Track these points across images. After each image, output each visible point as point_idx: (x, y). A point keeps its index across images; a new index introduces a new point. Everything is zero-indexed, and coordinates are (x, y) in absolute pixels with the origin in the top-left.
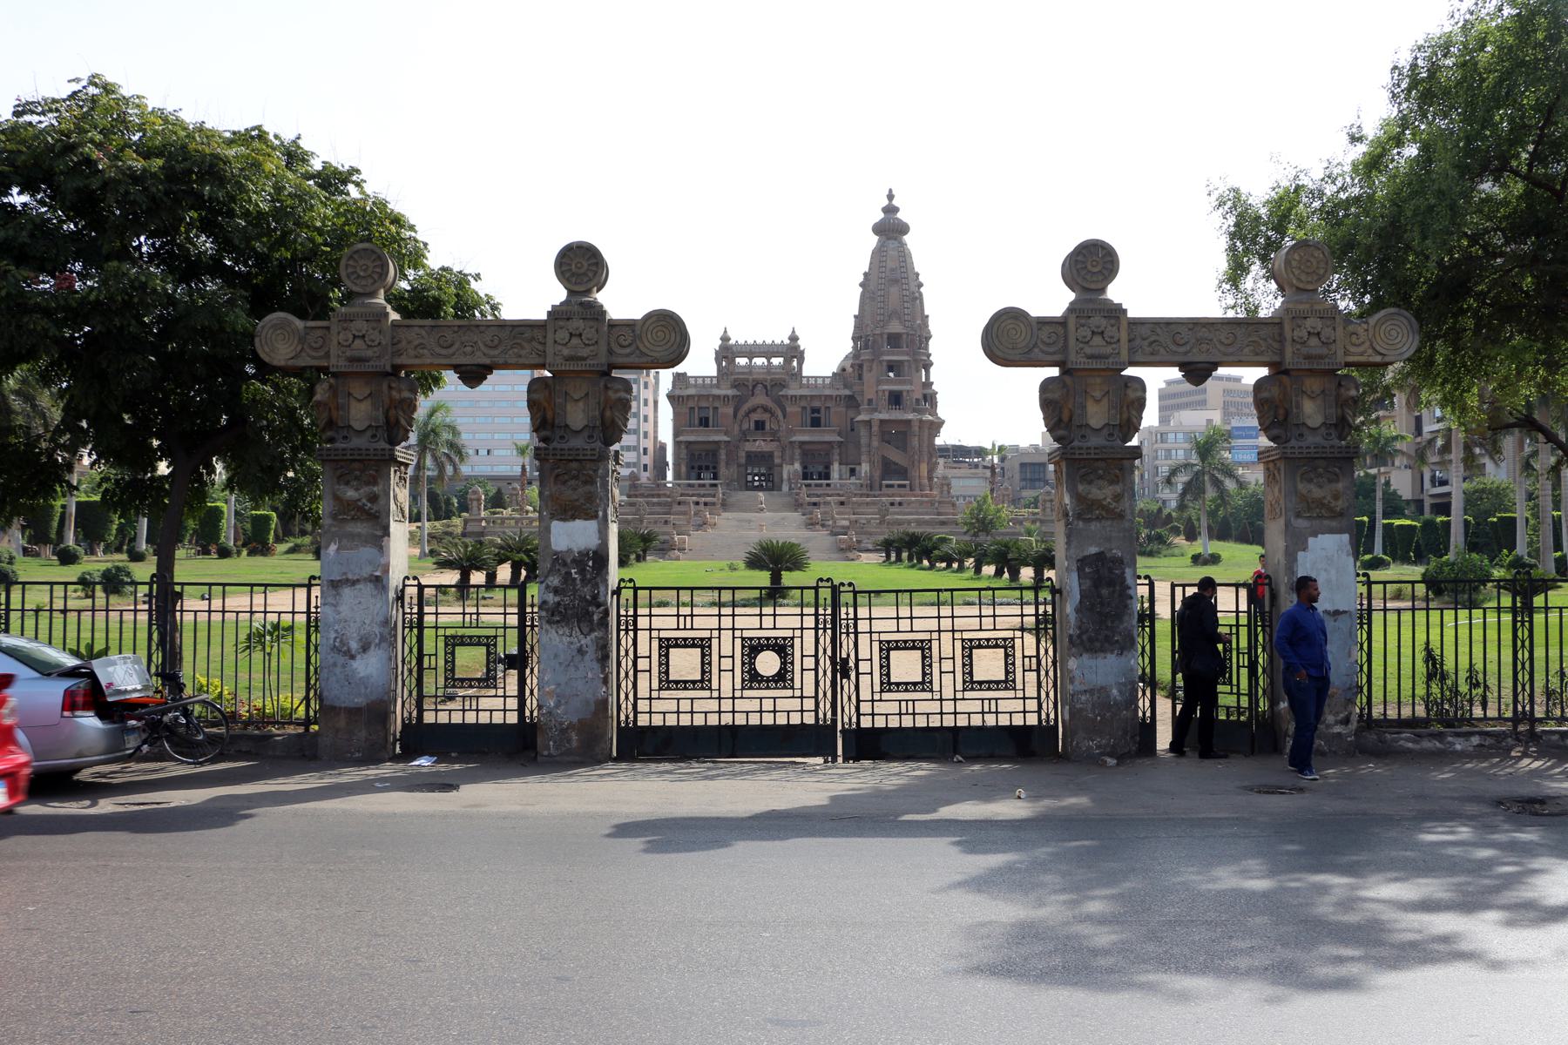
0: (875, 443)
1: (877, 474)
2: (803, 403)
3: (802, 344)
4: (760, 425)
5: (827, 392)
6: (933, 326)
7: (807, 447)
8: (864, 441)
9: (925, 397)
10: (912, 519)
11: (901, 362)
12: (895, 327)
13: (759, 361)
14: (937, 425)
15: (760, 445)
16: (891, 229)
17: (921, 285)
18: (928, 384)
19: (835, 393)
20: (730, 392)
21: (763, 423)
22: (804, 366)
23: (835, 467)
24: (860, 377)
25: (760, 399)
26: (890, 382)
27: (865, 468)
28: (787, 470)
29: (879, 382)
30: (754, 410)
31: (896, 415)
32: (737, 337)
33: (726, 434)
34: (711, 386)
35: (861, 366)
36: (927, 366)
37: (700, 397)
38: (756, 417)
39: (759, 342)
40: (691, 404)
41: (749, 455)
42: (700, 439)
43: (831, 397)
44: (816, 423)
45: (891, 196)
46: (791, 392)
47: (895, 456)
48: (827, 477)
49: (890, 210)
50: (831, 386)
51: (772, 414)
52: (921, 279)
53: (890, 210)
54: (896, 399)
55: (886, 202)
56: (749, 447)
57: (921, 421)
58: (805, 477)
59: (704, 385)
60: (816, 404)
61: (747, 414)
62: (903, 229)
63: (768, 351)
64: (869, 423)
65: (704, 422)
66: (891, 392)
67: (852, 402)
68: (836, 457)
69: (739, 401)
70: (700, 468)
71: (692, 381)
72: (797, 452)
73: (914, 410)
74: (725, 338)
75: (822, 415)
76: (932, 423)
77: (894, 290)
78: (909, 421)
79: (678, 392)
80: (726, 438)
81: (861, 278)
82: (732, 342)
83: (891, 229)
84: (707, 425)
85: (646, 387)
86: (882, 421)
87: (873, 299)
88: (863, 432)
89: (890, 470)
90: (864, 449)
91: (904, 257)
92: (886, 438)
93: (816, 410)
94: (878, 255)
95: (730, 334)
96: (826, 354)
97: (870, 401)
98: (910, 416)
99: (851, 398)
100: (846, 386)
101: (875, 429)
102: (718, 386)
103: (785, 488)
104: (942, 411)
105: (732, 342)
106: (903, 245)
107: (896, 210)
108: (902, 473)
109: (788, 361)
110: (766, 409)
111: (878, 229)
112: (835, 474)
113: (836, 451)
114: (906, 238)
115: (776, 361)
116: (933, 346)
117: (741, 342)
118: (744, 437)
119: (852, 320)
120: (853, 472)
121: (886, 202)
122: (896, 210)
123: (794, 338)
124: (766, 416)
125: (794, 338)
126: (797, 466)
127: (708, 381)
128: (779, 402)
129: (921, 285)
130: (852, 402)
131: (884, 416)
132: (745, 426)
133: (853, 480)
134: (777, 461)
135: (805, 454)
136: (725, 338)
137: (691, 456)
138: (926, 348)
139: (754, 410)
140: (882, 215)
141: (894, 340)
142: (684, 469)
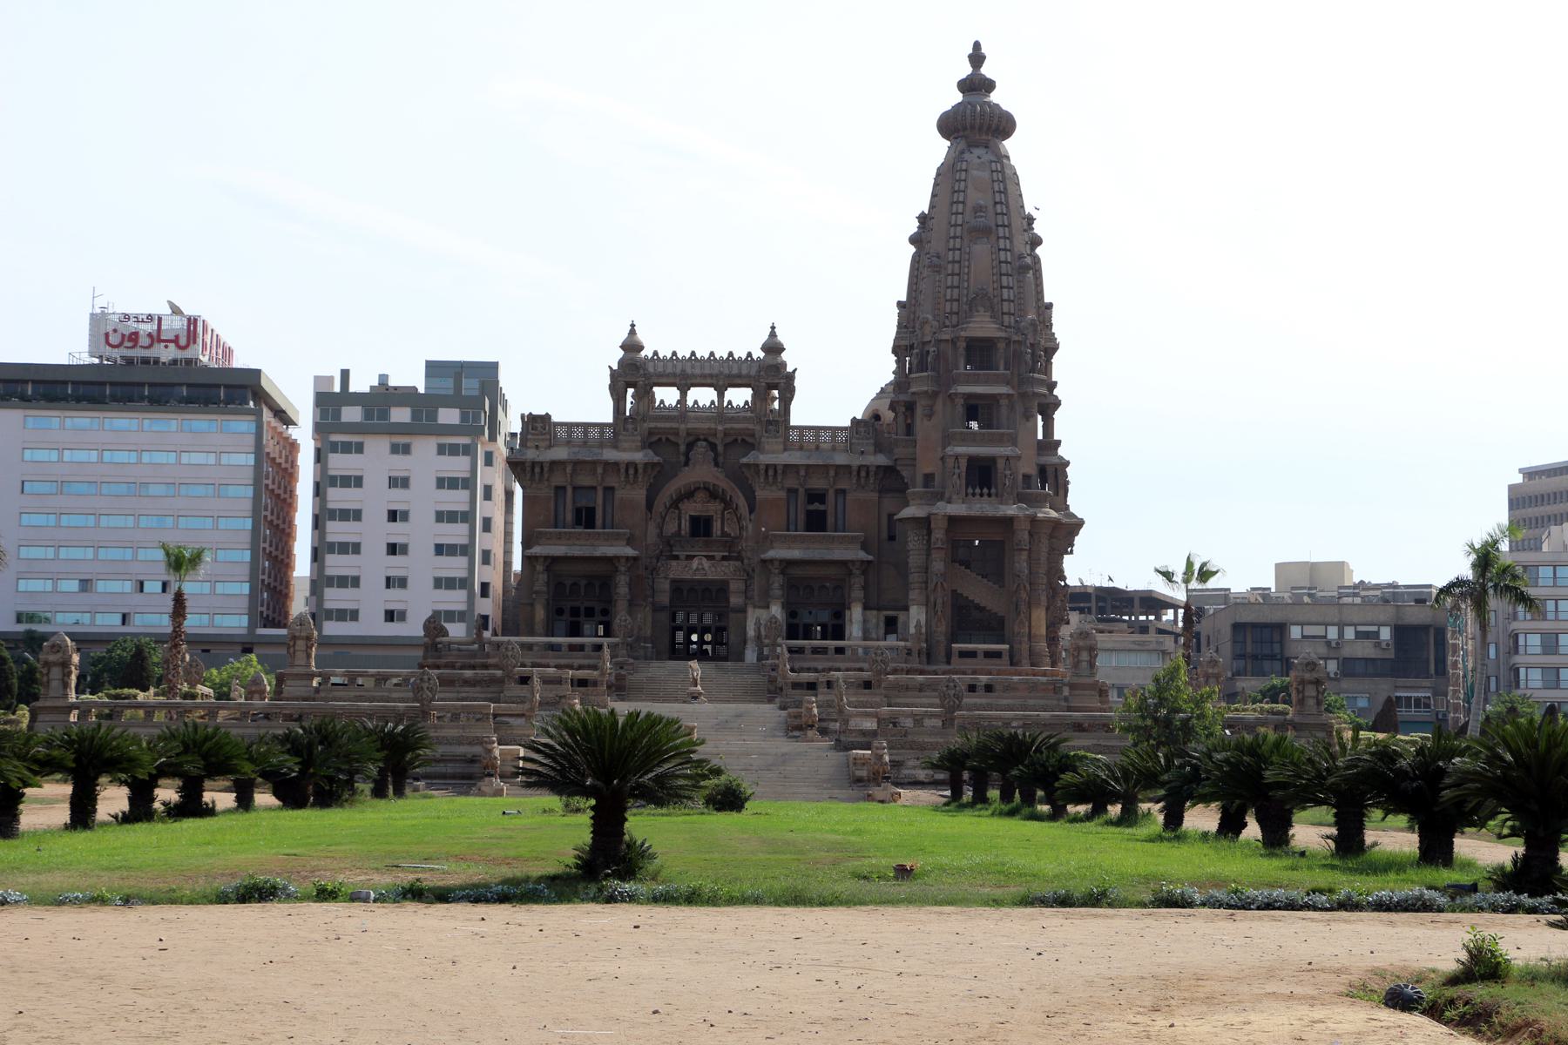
0: (938, 566)
1: (942, 629)
2: (791, 482)
3: (790, 359)
4: (701, 527)
5: (841, 459)
6: (1060, 326)
7: (797, 572)
8: (915, 560)
9: (1042, 470)
10: (1010, 713)
11: (994, 398)
12: (982, 326)
13: (702, 396)
14: (1067, 531)
15: (701, 567)
16: (976, 125)
17: (1037, 241)
18: (1051, 445)
19: (856, 461)
20: (639, 457)
21: (708, 522)
22: (795, 407)
23: (856, 614)
24: (909, 430)
25: (702, 471)
26: (973, 438)
27: (916, 616)
28: (754, 619)
29: (947, 439)
30: (689, 494)
31: (983, 507)
32: (658, 343)
33: (630, 541)
34: (601, 444)
35: (910, 407)
36: (1049, 407)
37: (577, 464)
38: (692, 508)
39: (702, 353)
40: (558, 479)
41: (677, 586)
42: (576, 551)
44: (816, 522)
45: (977, 58)
46: (764, 459)
47: (979, 592)
48: (838, 632)
49: (976, 85)
50: (850, 447)
51: (728, 504)
52: (1038, 228)
53: (976, 85)
54: (982, 475)
55: (967, 70)
56: (677, 570)
57: (1033, 520)
58: (792, 633)
60: (817, 483)
61: (675, 504)
62: (1003, 125)
63: (721, 373)
64: (925, 523)
65: (585, 518)
66: (973, 461)
67: (891, 480)
68: (857, 593)
69: (657, 475)
70: (575, 612)
71: (562, 433)
72: (777, 582)
73: (1020, 498)
74: (631, 346)
75: (829, 506)
76: (1056, 524)
77: (981, 249)
78: (1008, 522)
79: (531, 455)
80: (629, 552)
81: (913, 226)
82: (647, 352)
83: (976, 125)
84: (590, 524)
85: (489, 461)
86: (953, 520)
87: (937, 269)
88: (914, 542)
89: (968, 620)
90: (915, 578)
91: (1004, 183)
92: (960, 555)
93: (816, 497)
94: (948, 179)
95: (641, 336)
96: (842, 382)
97: (928, 478)
98: (1011, 510)
99: (889, 471)
100: (879, 448)
101: (938, 534)
102: (615, 444)
103: (751, 655)
104: (1077, 502)
105: (647, 352)
106: (1003, 158)
107: (989, 85)
108: (994, 627)
109: (761, 396)
110: (713, 494)
111: (949, 125)
112: (854, 629)
113: (858, 581)
114: (1009, 145)
115: (739, 396)
116: (1060, 367)
117: (665, 353)
118: (668, 548)
119: (894, 313)
120: (891, 625)
121: (967, 70)
122: (989, 85)
123: (773, 347)
124: (714, 508)
125: (773, 347)
126: (776, 610)
127: (594, 434)
128: (743, 478)
129: (1037, 241)
130: (891, 480)
131: (957, 509)
132: (671, 528)
133: (892, 641)
134: (735, 600)
135: (792, 586)
136: (631, 346)
137: (558, 589)
138: (1047, 369)
139: (689, 494)
140: (958, 97)
141: (980, 352)
142: (540, 613)
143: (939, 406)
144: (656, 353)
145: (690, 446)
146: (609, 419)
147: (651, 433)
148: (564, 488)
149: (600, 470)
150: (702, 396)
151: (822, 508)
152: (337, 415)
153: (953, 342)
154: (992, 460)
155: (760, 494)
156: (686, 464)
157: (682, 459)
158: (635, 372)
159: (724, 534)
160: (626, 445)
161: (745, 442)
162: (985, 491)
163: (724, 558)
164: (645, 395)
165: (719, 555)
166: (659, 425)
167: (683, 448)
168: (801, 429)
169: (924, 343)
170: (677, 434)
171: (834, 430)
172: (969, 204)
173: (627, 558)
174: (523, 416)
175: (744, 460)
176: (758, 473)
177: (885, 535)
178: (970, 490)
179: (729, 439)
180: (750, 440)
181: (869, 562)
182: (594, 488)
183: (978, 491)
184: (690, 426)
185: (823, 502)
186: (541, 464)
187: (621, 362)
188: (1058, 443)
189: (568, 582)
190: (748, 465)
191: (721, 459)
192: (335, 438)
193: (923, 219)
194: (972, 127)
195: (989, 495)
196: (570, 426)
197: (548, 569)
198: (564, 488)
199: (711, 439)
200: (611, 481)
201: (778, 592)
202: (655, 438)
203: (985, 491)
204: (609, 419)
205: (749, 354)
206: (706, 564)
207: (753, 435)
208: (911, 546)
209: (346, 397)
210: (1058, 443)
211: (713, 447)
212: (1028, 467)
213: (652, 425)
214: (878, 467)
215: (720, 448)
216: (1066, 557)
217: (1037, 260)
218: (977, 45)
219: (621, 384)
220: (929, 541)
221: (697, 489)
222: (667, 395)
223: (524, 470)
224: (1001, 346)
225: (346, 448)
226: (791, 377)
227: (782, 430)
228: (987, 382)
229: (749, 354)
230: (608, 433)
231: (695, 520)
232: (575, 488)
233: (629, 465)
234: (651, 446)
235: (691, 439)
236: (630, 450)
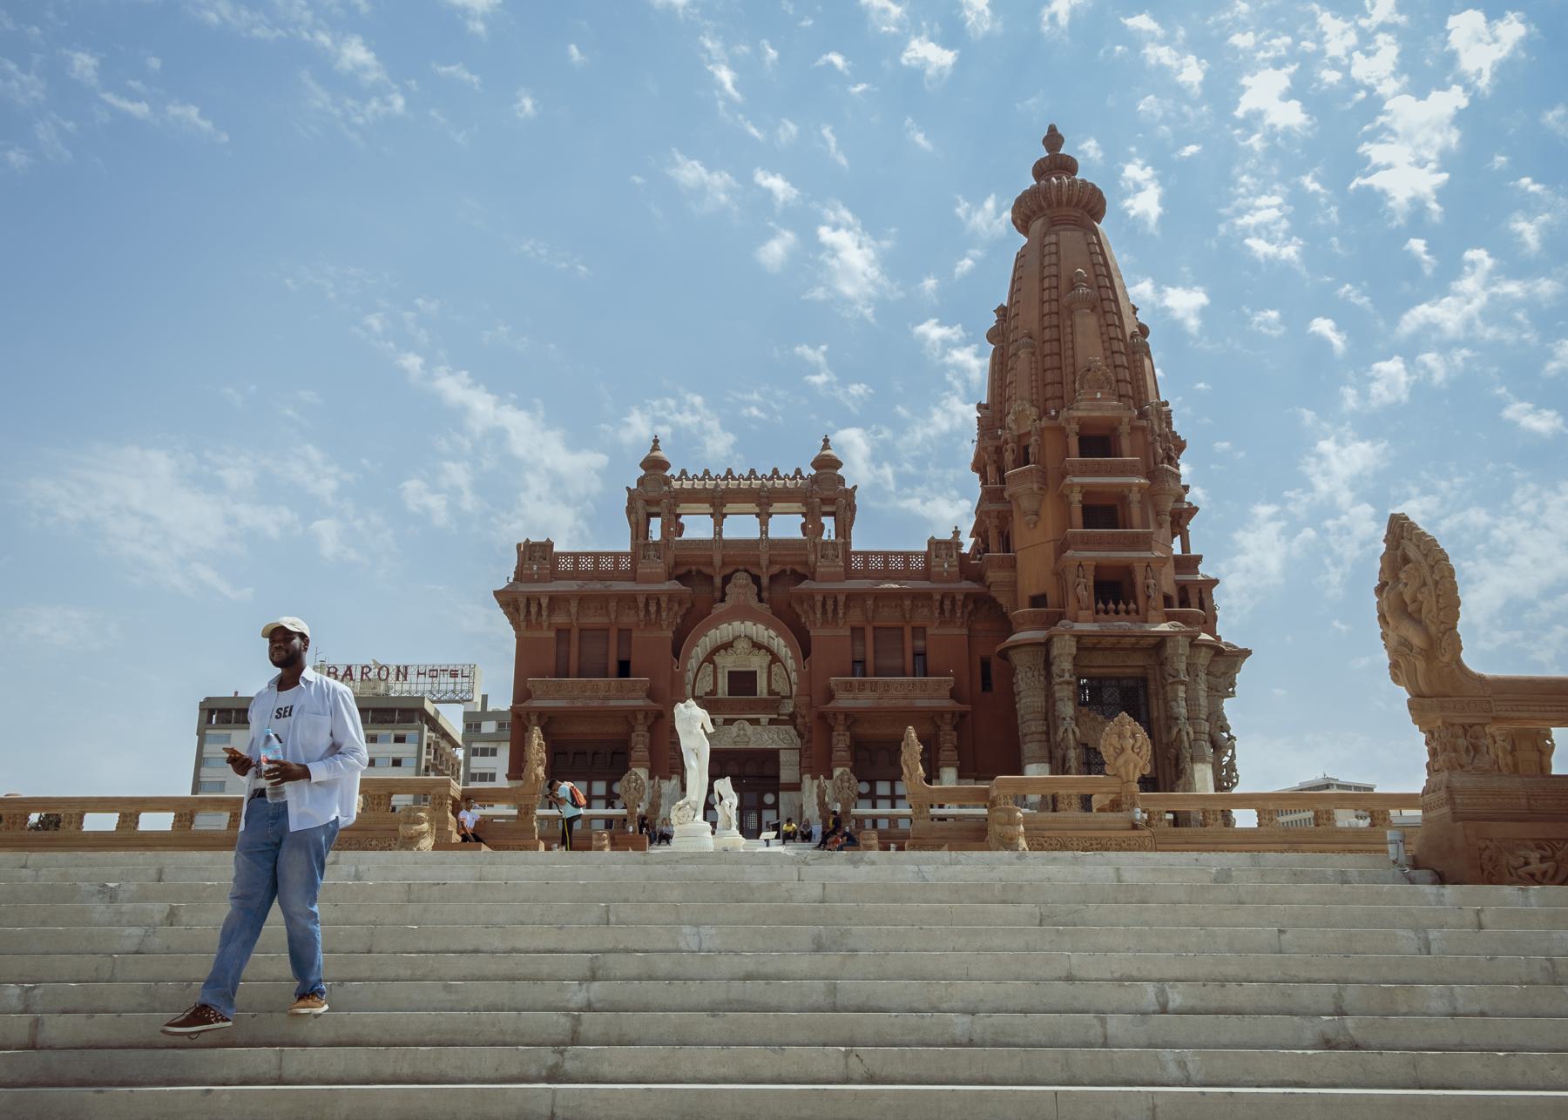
0: (1067, 709)
9: (1183, 589)
12: (1096, 406)
16: (1060, 207)
18: (1189, 563)
21: (751, 676)
36: (1180, 518)
37: (583, 599)
38: (727, 663)
43: (927, 596)
45: (1053, 139)
51: (775, 658)
59: (597, 575)
61: (709, 658)
63: (765, 498)
66: (1098, 568)
71: (565, 565)
73: (1169, 617)
74: (654, 465)
81: (992, 321)
83: (1060, 207)
96: (920, 498)
97: (1038, 601)
102: (632, 575)
105: (674, 471)
109: (812, 527)
122: (1069, 166)
123: (827, 464)
127: (606, 564)
136: (654, 465)
144: (684, 472)
145: (727, 579)
146: (626, 547)
149: (613, 604)
150: (741, 527)
152: (478, 726)
154: (1127, 570)
157: (718, 595)
158: (656, 492)
159: (771, 692)
162: (1122, 606)
163: (772, 722)
164: (674, 525)
165: (764, 718)
167: (718, 581)
168: (866, 555)
169: (1020, 437)
170: (711, 564)
171: (906, 556)
174: (519, 546)
176: (813, 608)
178: (1101, 606)
179: (776, 569)
180: (800, 569)
181: (963, 715)
183: (1111, 606)
187: (641, 481)
188: (1198, 559)
191: (765, 595)
192: (475, 745)
193: (1002, 312)
194: (1059, 203)
195: (1127, 612)
196: (576, 556)
199: (754, 571)
201: (846, 755)
202: (683, 570)
203: (1122, 606)
204: (628, 549)
205: (798, 471)
206: (749, 728)
207: (806, 563)
209: (485, 715)
210: (1198, 559)
212: (1168, 581)
214: (967, 596)
215: (765, 581)
217: (1147, 345)
218: (1052, 129)
219: (642, 516)
220: (1049, 676)
221: (737, 638)
222: (697, 527)
224: (1125, 429)
225: (484, 752)
226: (850, 494)
228: (1109, 473)
229: (798, 471)
230: (625, 565)
233: (649, 598)
234: (678, 578)
235: (728, 571)
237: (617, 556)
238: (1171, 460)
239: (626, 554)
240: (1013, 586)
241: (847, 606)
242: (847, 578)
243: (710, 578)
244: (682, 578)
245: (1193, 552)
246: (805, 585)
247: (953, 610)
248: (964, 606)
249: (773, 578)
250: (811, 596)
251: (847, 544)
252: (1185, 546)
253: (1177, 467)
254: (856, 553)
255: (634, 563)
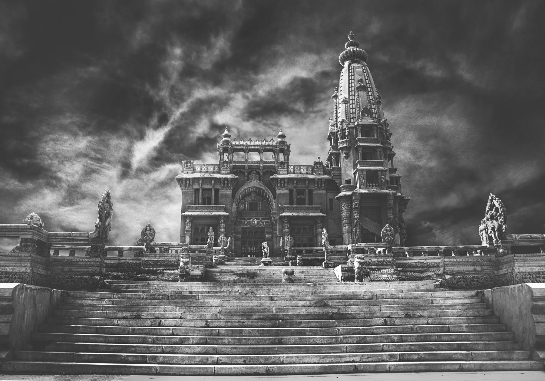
3: (287, 140)
9: (391, 178)
19: (317, 177)
25: (254, 183)
30: (249, 194)
33: (225, 210)
35: (338, 155)
37: (204, 179)
40: (196, 186)
42: (203, 214)
44: (301, 202)
60: (301, 187)
61: (244, 197)
65: (207, 201)
69: (236, 185)
80: (225, 214)
97: (348, 182)
128: (272, 184)
132: (242, 207)
141: (367, 130)
143: (351, 154)
145: (249, 173)
147: (234, 167)
148: (199, 190)
151: (303, 197)
153: (356, 127)
155: (278, 191)
156: (248, 180)
157: (246, 178)
160: (223, 172)
161: (273, 170)
163: (263, 219)
166: (237, 164)
167: (246, 174)
168: (294, 166)
172: (356, 79)
173: (224, 216)
175: (272, 177)
176: (277, 183)
177: (329, 207)
182: (211, 190)
184: (249, 165)
185: (303, 195)
186: (189, 179)
189: (200, 228)
190: (273, 179)
191: (262, 178)
195: (376, 186)
197: (191, 221)
198: (199, 190)
200: (218, 186)
202: (235, 170)
208: (343, 208)
211: (258, 173)
213: (234, 164)
215: (261, 174)
216: (403, 214)
220: (352, 205)
223: (182, 182)
226: (288, 146)
227: (286, 166)
231: (250, 204)
232: (204, 190)
235: (250, 170)
236: (226, 174)
237: (214, 165)
238: (388, 138)
239: (217, 165)
240: (340, 176)
241: (288, 183)
242: (288, 174)
243: (244, 173)
244: (235, 173)
245: (394, 167)
246: (274, 176)
247: (321, 184)
248: (325, 183)
249: (264, 173)
250: (277, 179)
251: (288, 163)
252: (392, 166)
253: (390, 140)
254: (291, 166)
255: (219, 168)
